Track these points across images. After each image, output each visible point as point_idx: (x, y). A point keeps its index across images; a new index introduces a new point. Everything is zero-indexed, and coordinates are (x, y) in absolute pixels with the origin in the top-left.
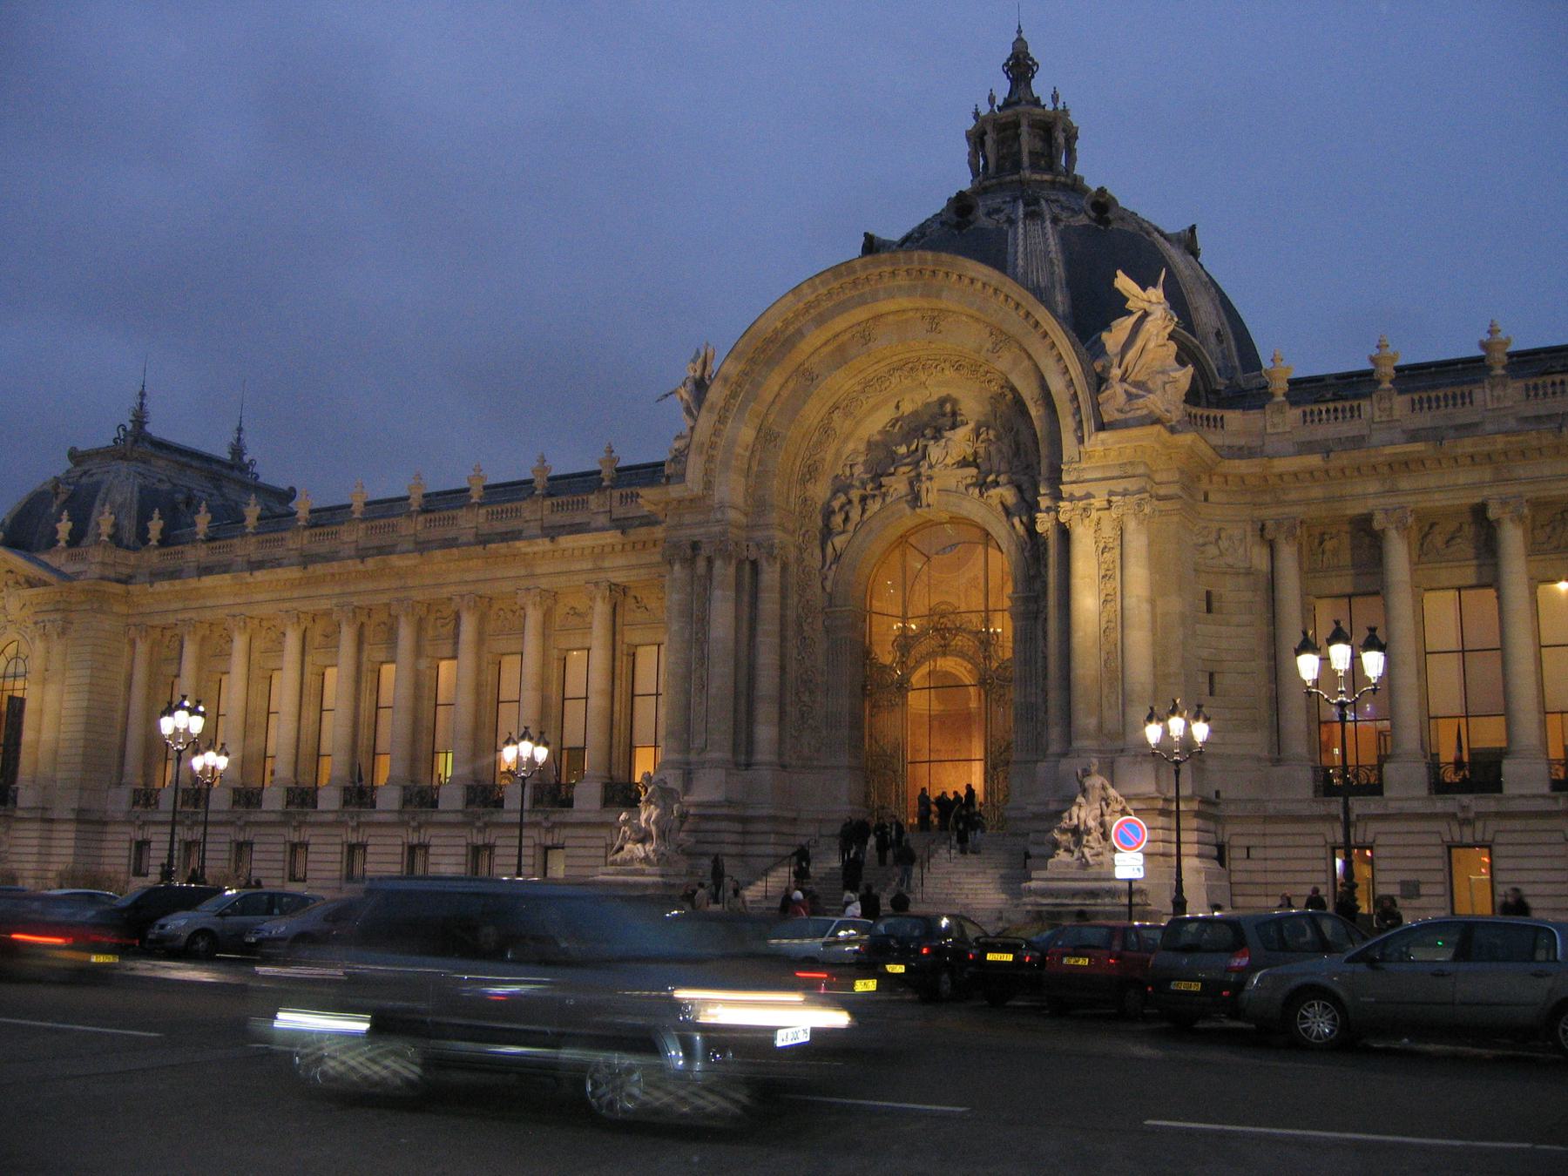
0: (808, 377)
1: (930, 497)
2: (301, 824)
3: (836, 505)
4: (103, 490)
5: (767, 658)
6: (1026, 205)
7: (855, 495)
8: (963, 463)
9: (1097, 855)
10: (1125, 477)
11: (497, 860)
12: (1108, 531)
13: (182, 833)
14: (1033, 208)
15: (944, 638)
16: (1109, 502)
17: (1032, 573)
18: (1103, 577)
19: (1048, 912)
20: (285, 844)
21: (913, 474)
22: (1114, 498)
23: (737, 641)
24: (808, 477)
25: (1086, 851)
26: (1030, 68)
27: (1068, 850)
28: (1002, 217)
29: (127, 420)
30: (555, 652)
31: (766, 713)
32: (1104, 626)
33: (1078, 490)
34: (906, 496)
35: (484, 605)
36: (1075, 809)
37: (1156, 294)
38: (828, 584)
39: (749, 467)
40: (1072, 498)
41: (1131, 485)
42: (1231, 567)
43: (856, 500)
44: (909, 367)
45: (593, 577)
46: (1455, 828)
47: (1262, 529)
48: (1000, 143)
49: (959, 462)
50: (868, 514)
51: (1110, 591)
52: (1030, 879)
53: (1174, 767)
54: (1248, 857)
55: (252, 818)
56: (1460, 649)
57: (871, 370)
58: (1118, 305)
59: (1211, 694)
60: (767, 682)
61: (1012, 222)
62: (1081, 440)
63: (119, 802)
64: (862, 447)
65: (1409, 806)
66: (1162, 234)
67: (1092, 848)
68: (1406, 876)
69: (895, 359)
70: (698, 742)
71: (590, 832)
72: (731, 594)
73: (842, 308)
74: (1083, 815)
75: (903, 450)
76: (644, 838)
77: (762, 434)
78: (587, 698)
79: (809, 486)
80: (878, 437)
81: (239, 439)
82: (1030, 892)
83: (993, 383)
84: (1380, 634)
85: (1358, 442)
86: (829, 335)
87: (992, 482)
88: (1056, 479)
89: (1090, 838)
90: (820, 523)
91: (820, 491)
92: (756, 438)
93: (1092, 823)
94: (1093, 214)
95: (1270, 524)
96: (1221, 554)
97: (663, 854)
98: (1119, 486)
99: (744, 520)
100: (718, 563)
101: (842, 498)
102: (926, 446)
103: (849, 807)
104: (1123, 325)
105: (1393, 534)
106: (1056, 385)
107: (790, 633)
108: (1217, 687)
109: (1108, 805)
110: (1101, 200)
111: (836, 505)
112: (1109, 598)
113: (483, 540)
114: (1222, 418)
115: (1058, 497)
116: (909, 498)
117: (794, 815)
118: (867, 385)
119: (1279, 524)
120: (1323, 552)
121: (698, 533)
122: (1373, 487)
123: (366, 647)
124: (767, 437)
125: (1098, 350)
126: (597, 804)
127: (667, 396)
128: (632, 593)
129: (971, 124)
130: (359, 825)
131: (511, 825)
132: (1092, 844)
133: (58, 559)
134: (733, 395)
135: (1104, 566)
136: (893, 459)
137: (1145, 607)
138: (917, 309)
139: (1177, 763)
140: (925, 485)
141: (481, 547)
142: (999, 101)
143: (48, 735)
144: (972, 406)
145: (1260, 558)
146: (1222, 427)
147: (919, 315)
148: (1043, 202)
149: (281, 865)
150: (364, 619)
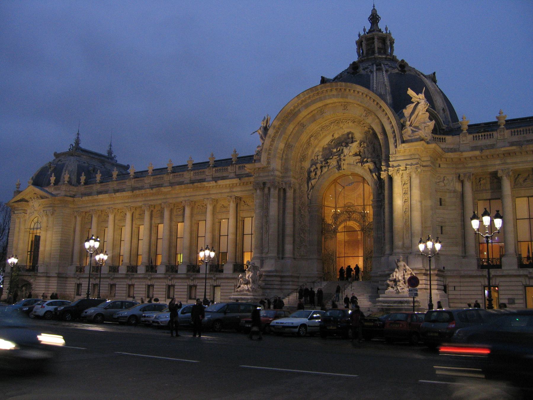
0: (302, 126)
1: (344, 167)
2: (132, 278)
3: (312, 169)
4: (66, 166)
5: (289, 221)
6: (377, 66)
7: (319, 166)
8: (356, 155)
9: (402, 289)
11: (198, 290)
12: (406, 178)
13: (92, 281)
14: (379, 67)
15: (349, 214)
16: (406, 168)
17: (380, 192)
18: (404, 193)
19: (385, 308)
20: (127, 285)
21: (338, 159)
22: (407, 166)
23: (278, 216)
24: (302, 160)
25: (398, 287)
26: (378, 19)
27: (392, 287)
28: (368, 70)
29: (73, 142)
30: (217, 220)
31: (289, 240)
32: (404, 210)
33: (395, 164)
35: (193, 204)
36: (394, 273)
37: (422, 96)
38: (310, 196)
39: (283, 157)
40: (393, 167)
41: (414, 162)
42: (448, 190)
43: (319, 168)
44: (337, 122)
45: (230, 194)
46: (527, 280)
47: (459, 177)
48: (367, 45)
49: (354, 154)
51: (407, 199)
52: (379, 297)
53: (429, 258)
54: (455, 290)
55: (116, 276)
56: (529, 218)
57: (324, 123)
58: (409, 100)
59: (442, 233)
60: (289, 230)
61: (372, 72)
62: (396, 147)
63: (71, 270)
64: (321, 150)
65: (511, 272)
66: (424, 75)
67: (401, 287)
68: (510, 297)
69: (332, 119)
70: (266, 250)
71: (229, 281)
72: (277, 200)
73: (314, 102)
74: (397, 275)
75: (335, 150)
76: (247, 283)
77: (287, 145)
78: (228, 235)
79: (303, 163)
80: (326, 146)
81: (110, 149)
82: (379, 301)
83: (366, 127)
84: (500, 213)
85: (492, 146)
86: (309, 111)
87: (365, 161)
88: (387, 160)
89: (400, 283)
90: (307, 176)
91: (307, 165)
92: (285, 147)
93: (400, 278)
94: (400, 69)
95: (462, 175)
96: (445, 185)
97: (254, 288)
98: (409, 162)
99: (281, 175)
100: (272, 190)
101: (314, 167)
102: (343, 149)
103: (317, 273)
104: (410, 107)
105: (505, 178)
106: (388, 128)
107: (297, 213)
108: (444, 231)
109: (406, 272)
110: (403, 64)
111: (312, 169)
112: (406, 201)
113: (192, 182)
114: (445, 139)
115: (388, 166)
116: (337, 167)
117: (298, 275)
118: (322, 128)
119: (465, 175)
120: (480, 185)
121: (265, 179)
122: (498, 162)
123: (153, 218)
124: (288, 146)
125: (402, 116)
126: (231, 272)
127: (254, 133)
128: (243, 200)
129: (357, 38)
130: (151, 279)
131: (202, 278)
132: (401, 285)
133: (51, 189)
134: (277, 132)
135: (404, 190)
136: (332, 154)
137: (419, 204)
138: (339, 102)
139: (430, 257)
140: (343, 162)
141: (192, 184)
142: (367, 31)
143: (48, 248)
144: (358, 135)
145: (458, 187)
146: (445, 141)
147: (340, 104)
148: (382, 65)
149: (125, 292)
150: (152, 209)
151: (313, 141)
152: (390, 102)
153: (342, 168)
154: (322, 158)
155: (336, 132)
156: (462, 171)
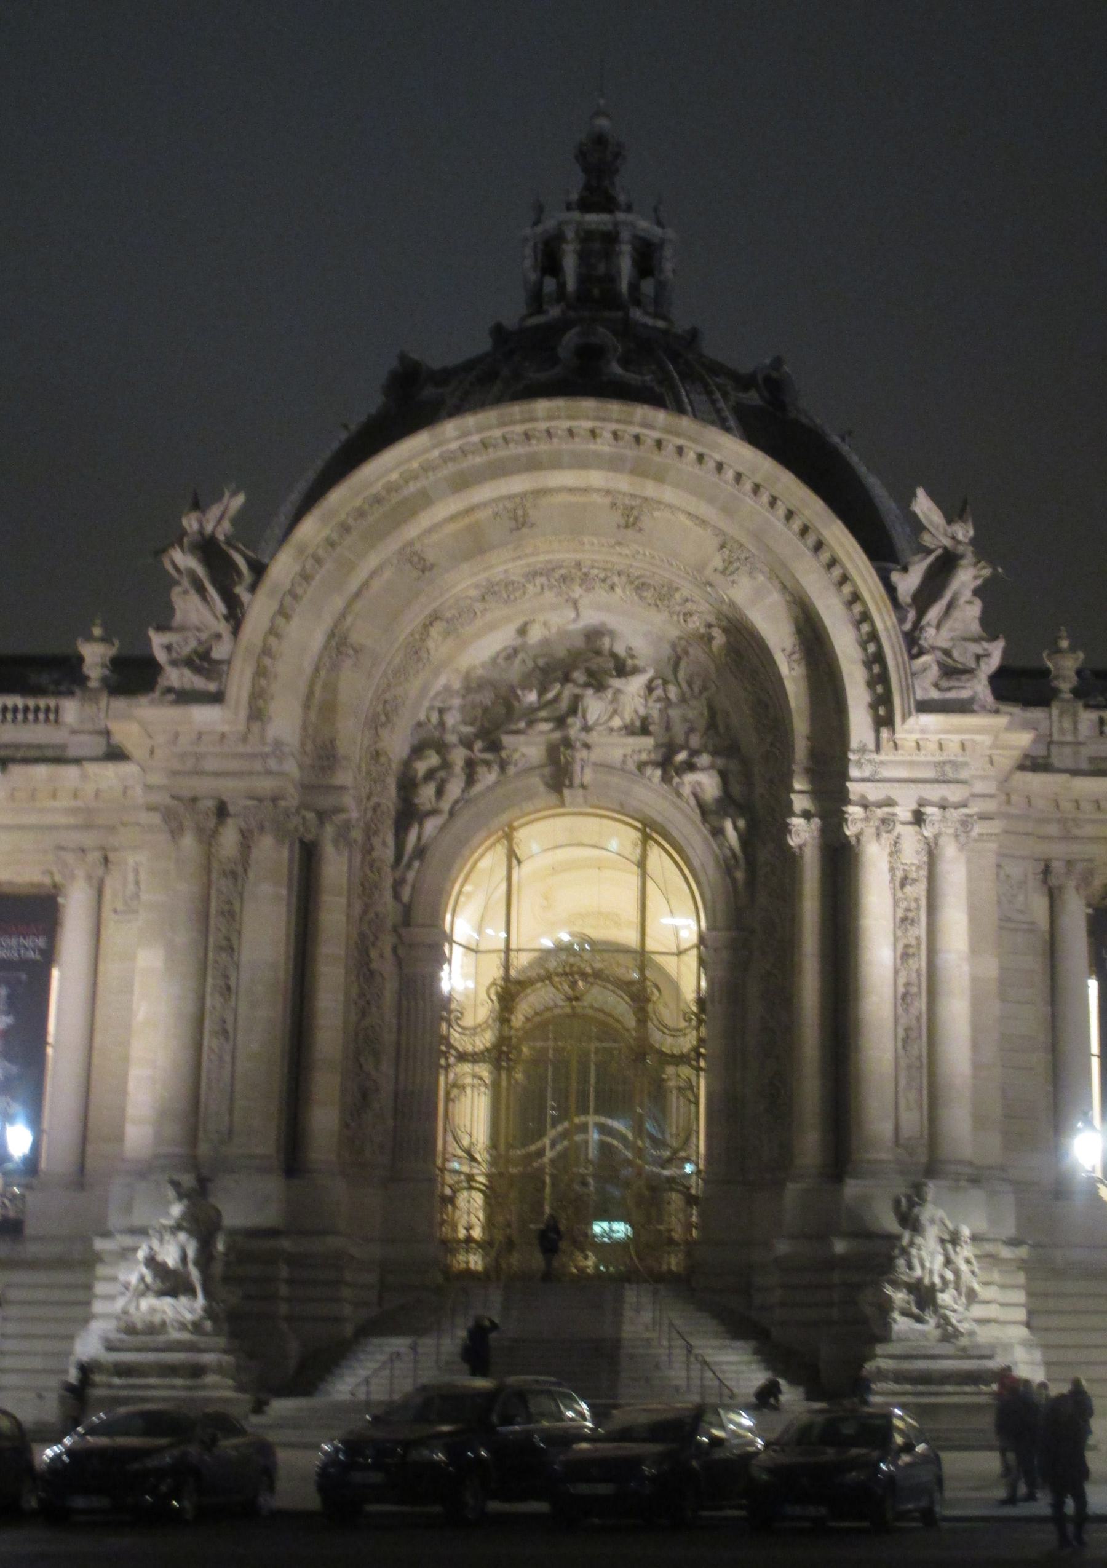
7: (458, 756)
8: (630, 730)
10: (944, 782)
15: (573, 985)
18: (904, 920)
21: (557, 735)
22: (928, 810)
24: (383, 718)
27: (905, 1313)
32: (901, 990)
33: (873, 792)
34: (542, 766)
38: (406, 893)
41: (954, 793)
47: (1047, 871)
50: (478, 788)
51: (913, 942)
64: (457, 685)
73: (499, 470)
87: (683, 763)
95: (1057, 866)
98: (934, 793)
110: (774, 374)
111: (421, 767)
134: (305, 577)
135: (903, 905)
137: (966, 968)
147: (607, 501)
151: (438, 646)
152: (234, 494)
153: (577, 781)
154: (465, 723)
155: (541, 618)
156: (1058, 851)
